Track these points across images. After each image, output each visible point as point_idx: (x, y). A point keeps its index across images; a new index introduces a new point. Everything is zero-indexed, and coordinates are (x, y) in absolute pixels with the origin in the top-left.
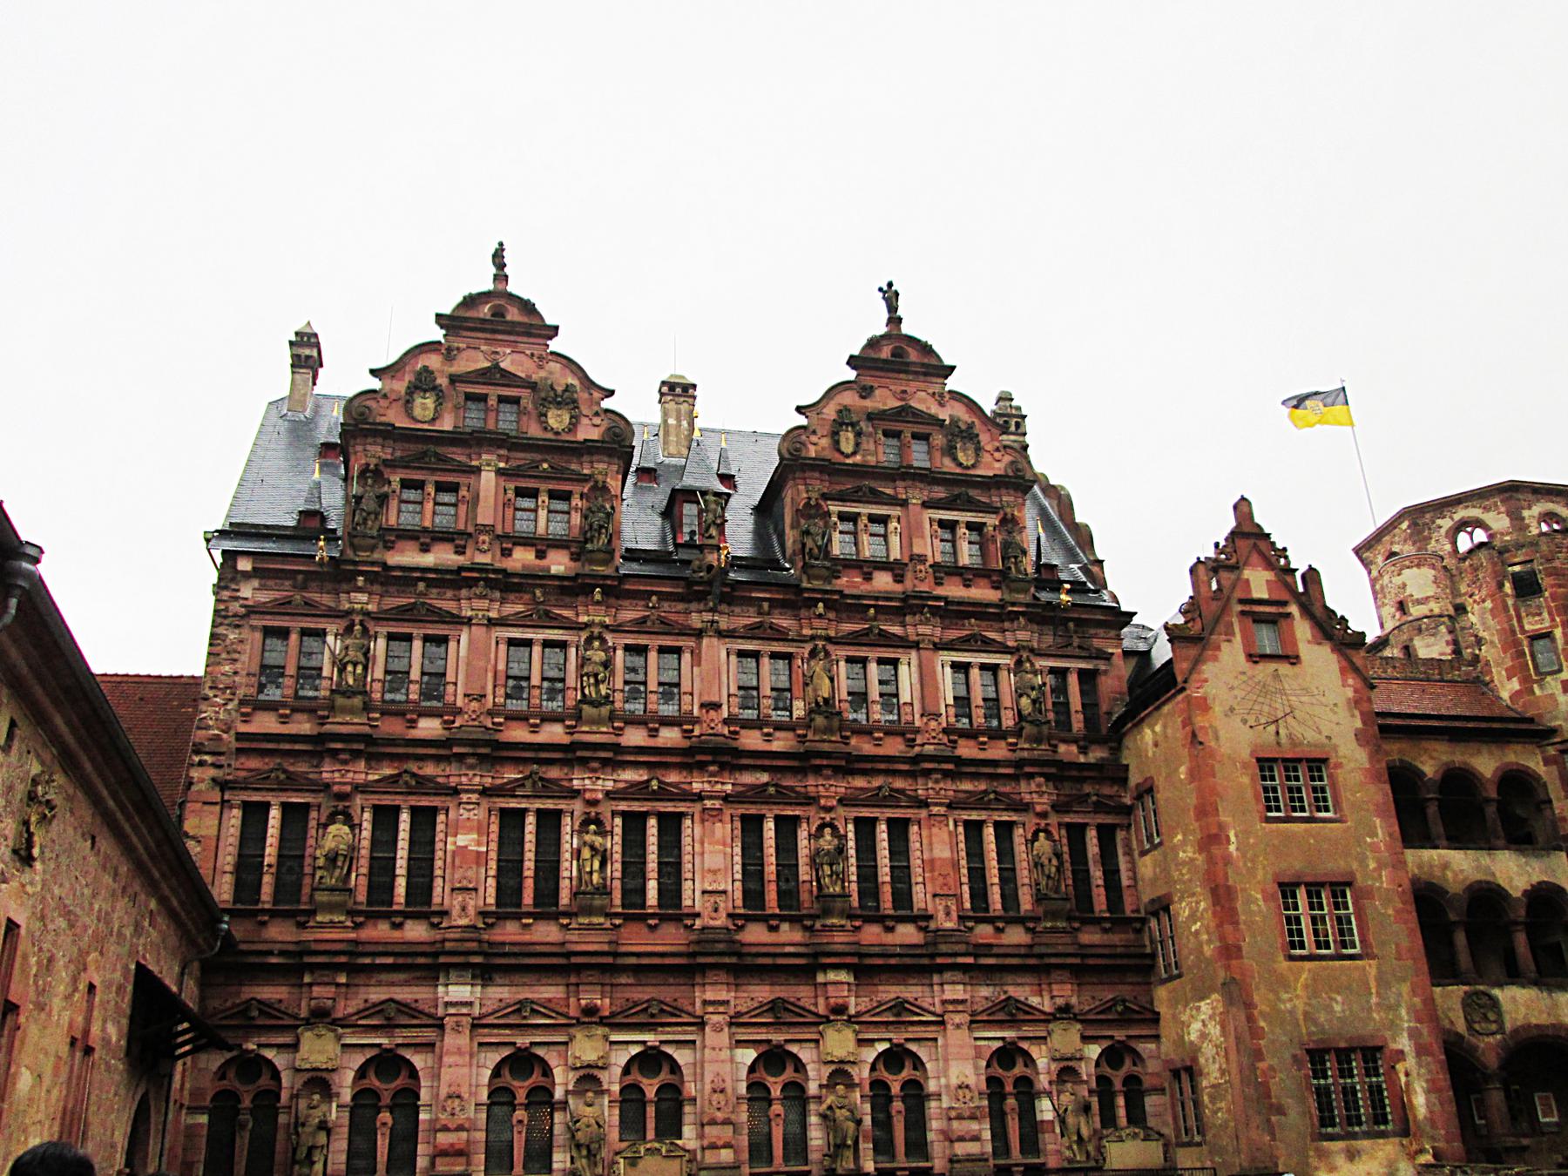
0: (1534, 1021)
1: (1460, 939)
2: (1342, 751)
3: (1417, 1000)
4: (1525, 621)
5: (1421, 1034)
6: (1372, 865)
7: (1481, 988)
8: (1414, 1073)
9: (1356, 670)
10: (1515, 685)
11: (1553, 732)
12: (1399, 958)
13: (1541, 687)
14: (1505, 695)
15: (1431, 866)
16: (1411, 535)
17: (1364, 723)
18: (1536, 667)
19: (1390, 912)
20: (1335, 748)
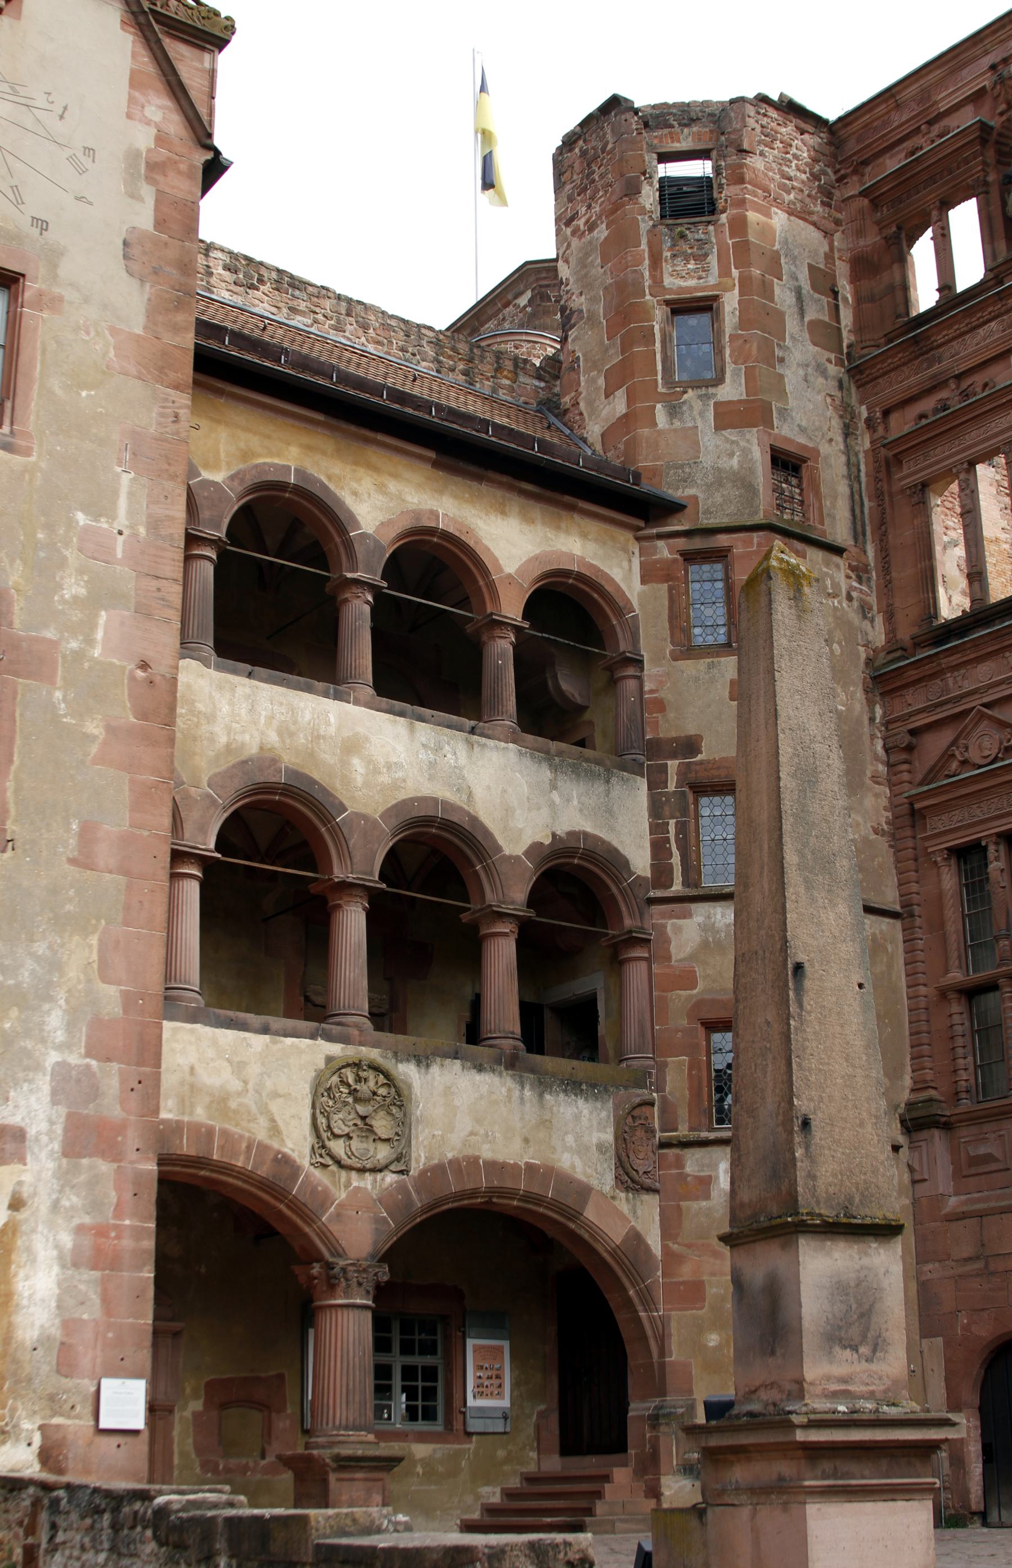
0: (486, 1153)
1: (352, 924)
2: (66, 269)
3: (111, 996)
4: (667, 268)
5: (94, 1093)
6: (73, 587)
7: (373, 1054)
8: (41, 1204)
9: (176, 89)
10: (619, 405)
11: (673, 508)
12: (84, 861)
13: (673, 412)
14: (594, 431)
15: (317, 738)
16: (533, 315)
17: (160, 223)
18: (667, 370)
19: (94, 728)
20: (54, 256)
